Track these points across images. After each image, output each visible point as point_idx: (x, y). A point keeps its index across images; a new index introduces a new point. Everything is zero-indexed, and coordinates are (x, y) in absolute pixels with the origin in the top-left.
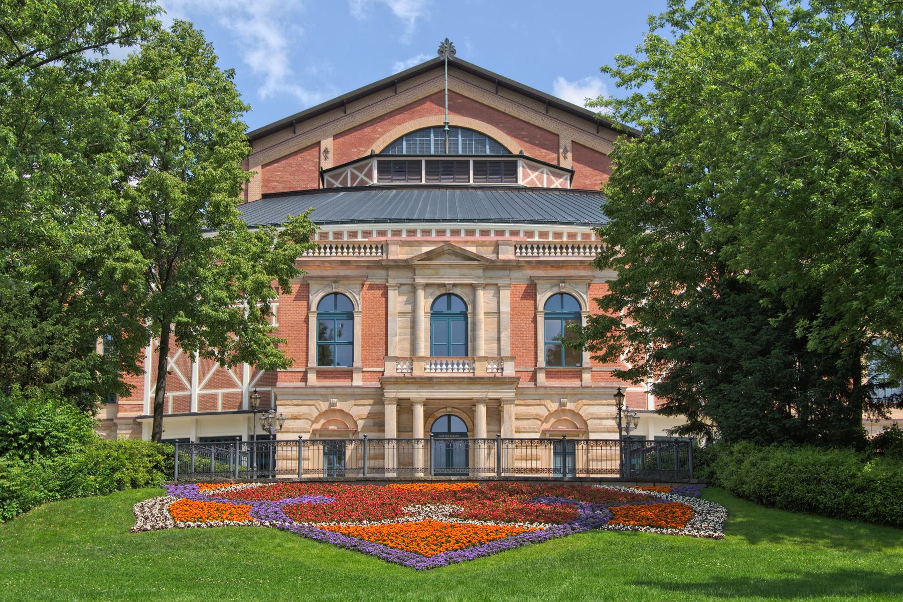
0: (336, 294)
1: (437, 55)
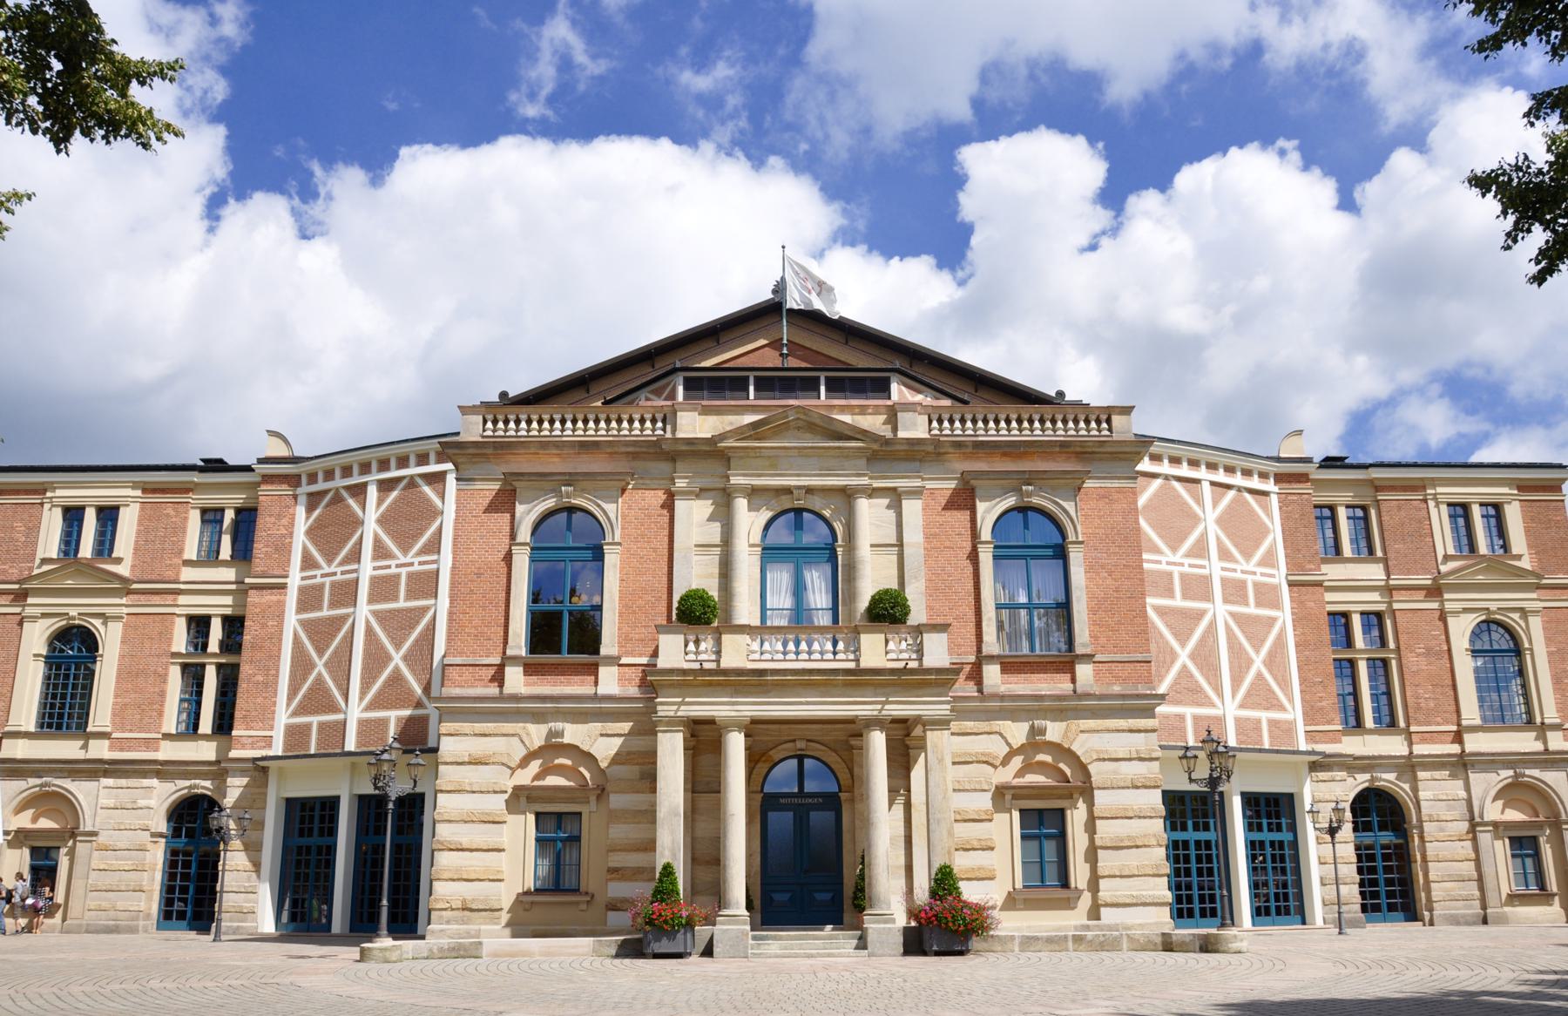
1: (771, 296)
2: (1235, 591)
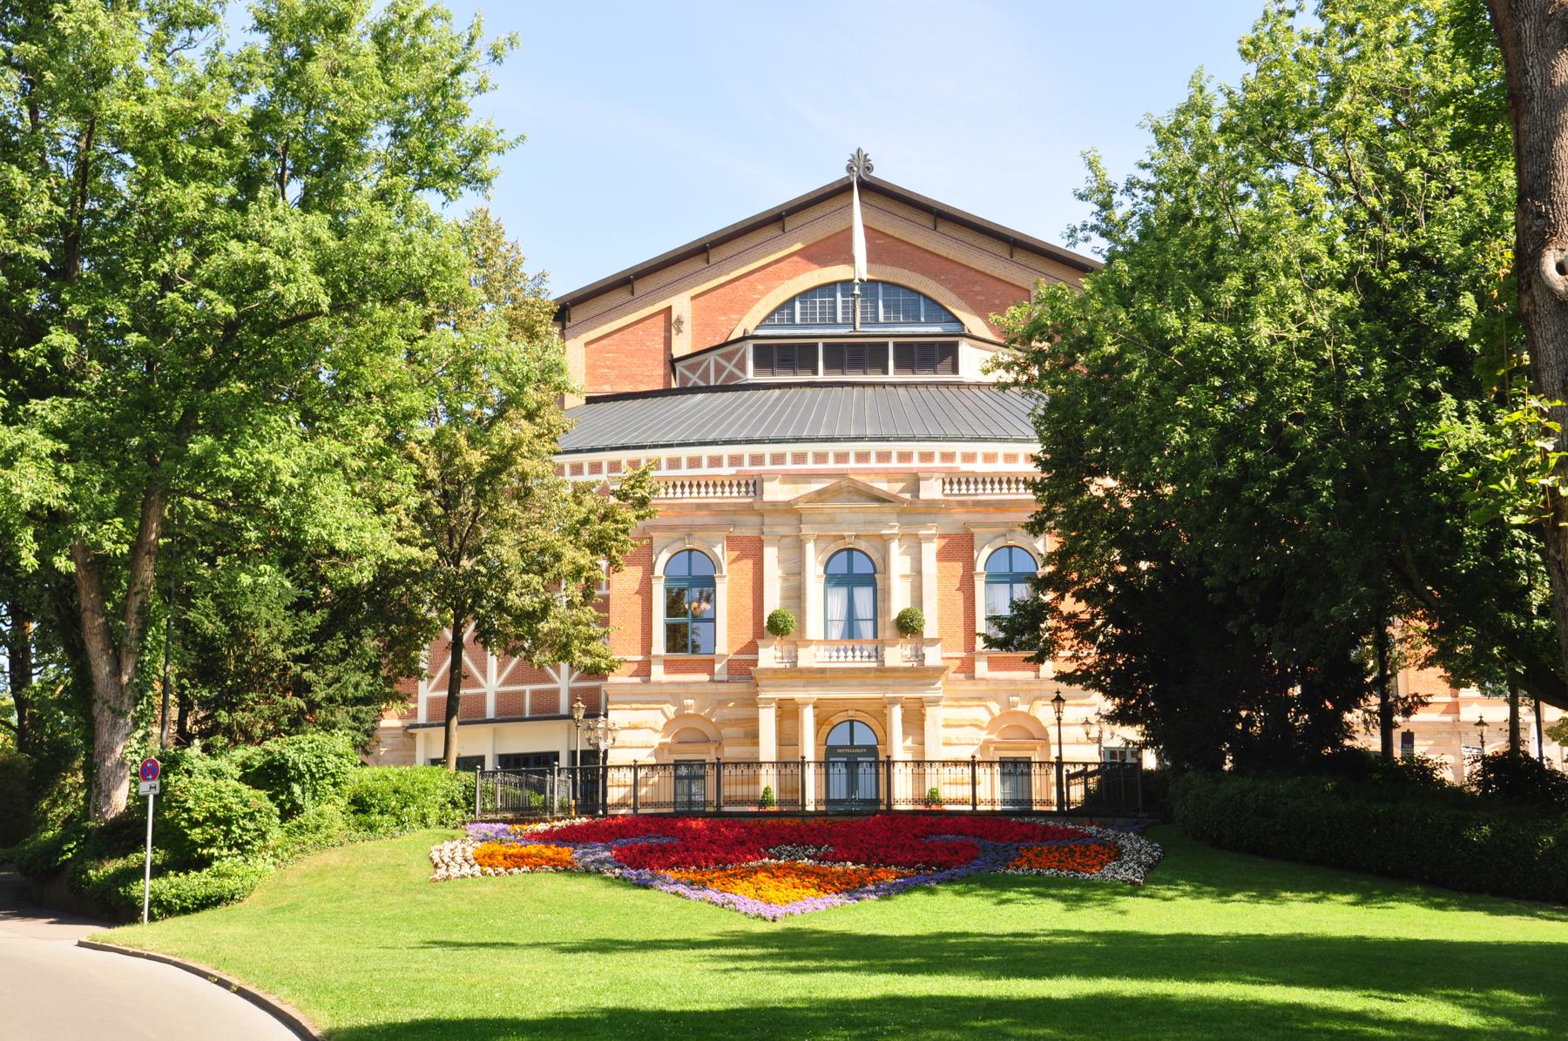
0: (690, 551)
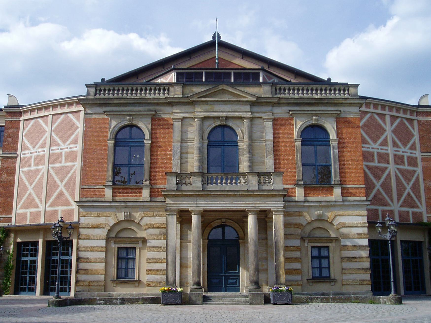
2: (399, 160)
